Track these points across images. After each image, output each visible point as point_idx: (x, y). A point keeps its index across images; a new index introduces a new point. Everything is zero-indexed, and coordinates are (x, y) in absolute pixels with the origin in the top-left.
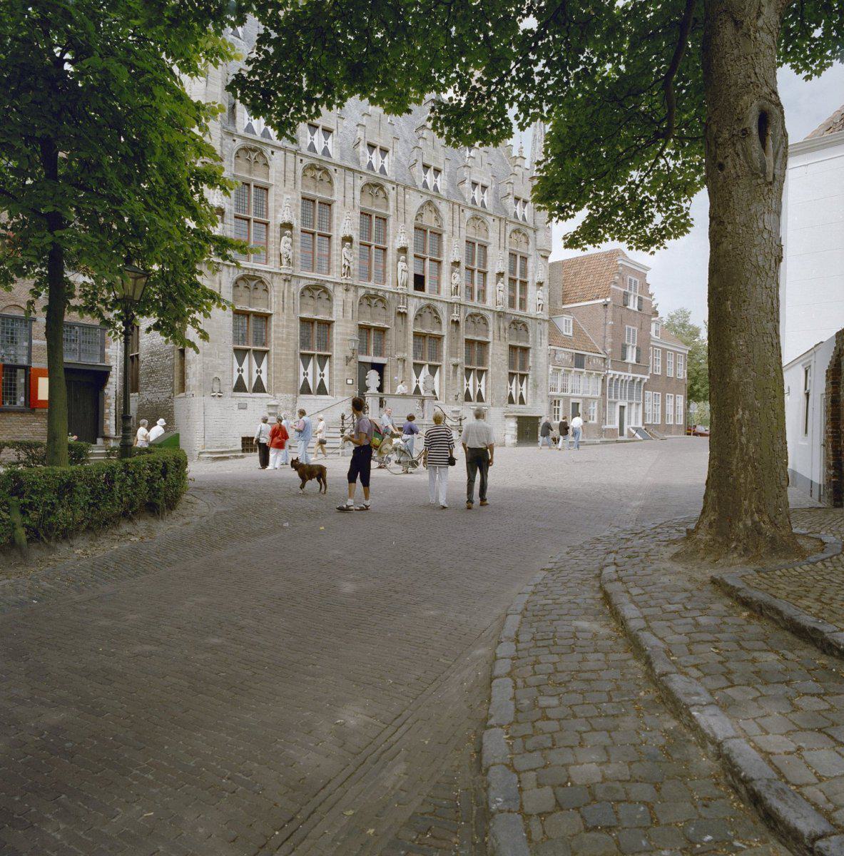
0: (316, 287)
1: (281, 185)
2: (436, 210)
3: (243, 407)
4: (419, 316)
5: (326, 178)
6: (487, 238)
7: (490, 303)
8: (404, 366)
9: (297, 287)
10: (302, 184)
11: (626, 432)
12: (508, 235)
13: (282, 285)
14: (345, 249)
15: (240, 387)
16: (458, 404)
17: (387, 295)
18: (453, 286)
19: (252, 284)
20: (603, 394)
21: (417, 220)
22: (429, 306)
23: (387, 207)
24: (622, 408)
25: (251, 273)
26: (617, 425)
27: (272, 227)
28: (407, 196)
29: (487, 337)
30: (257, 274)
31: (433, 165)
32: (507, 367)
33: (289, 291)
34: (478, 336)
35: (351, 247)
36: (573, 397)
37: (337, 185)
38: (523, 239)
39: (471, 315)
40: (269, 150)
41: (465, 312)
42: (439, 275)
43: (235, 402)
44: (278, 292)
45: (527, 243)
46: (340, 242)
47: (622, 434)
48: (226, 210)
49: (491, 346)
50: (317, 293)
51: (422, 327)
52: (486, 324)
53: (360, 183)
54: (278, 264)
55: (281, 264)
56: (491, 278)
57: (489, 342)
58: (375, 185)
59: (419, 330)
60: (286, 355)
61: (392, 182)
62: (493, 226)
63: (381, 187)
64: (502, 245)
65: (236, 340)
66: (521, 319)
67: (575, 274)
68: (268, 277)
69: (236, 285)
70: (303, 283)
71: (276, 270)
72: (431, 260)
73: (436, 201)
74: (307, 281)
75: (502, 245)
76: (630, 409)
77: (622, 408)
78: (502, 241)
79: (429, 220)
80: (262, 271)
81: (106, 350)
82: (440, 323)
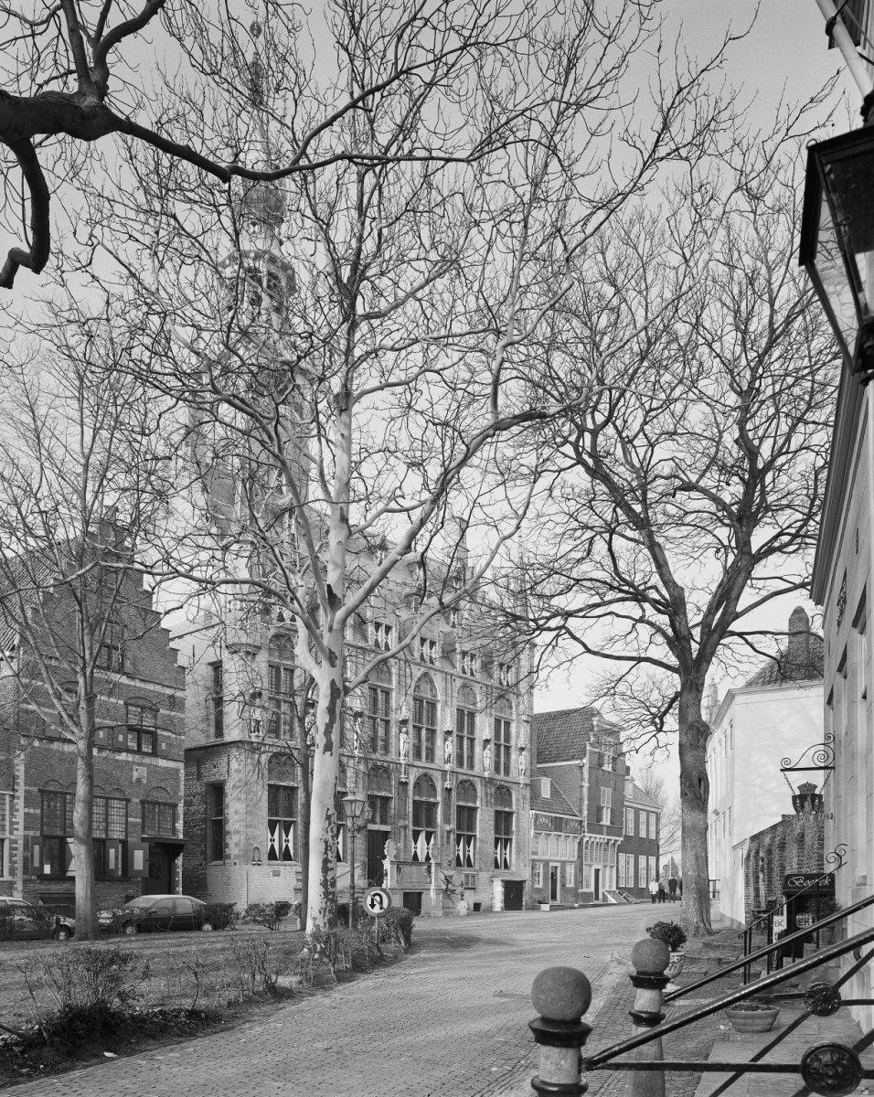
3: (276, 874)
4: (417, 784)
7: (477, 770)
11: (601, 896)
15: (272, 856)
20: (580, 857)
22: (425, 775)
24: (597, 871)
26: (592, 889)
34: (468, 802)
43: (270, 869)
47: (597, 898)
51: (419, 795)
52: (475, 790)
59: (417, 798)
76: (604, 872)
77: (597, 871)
82: (435, 790)
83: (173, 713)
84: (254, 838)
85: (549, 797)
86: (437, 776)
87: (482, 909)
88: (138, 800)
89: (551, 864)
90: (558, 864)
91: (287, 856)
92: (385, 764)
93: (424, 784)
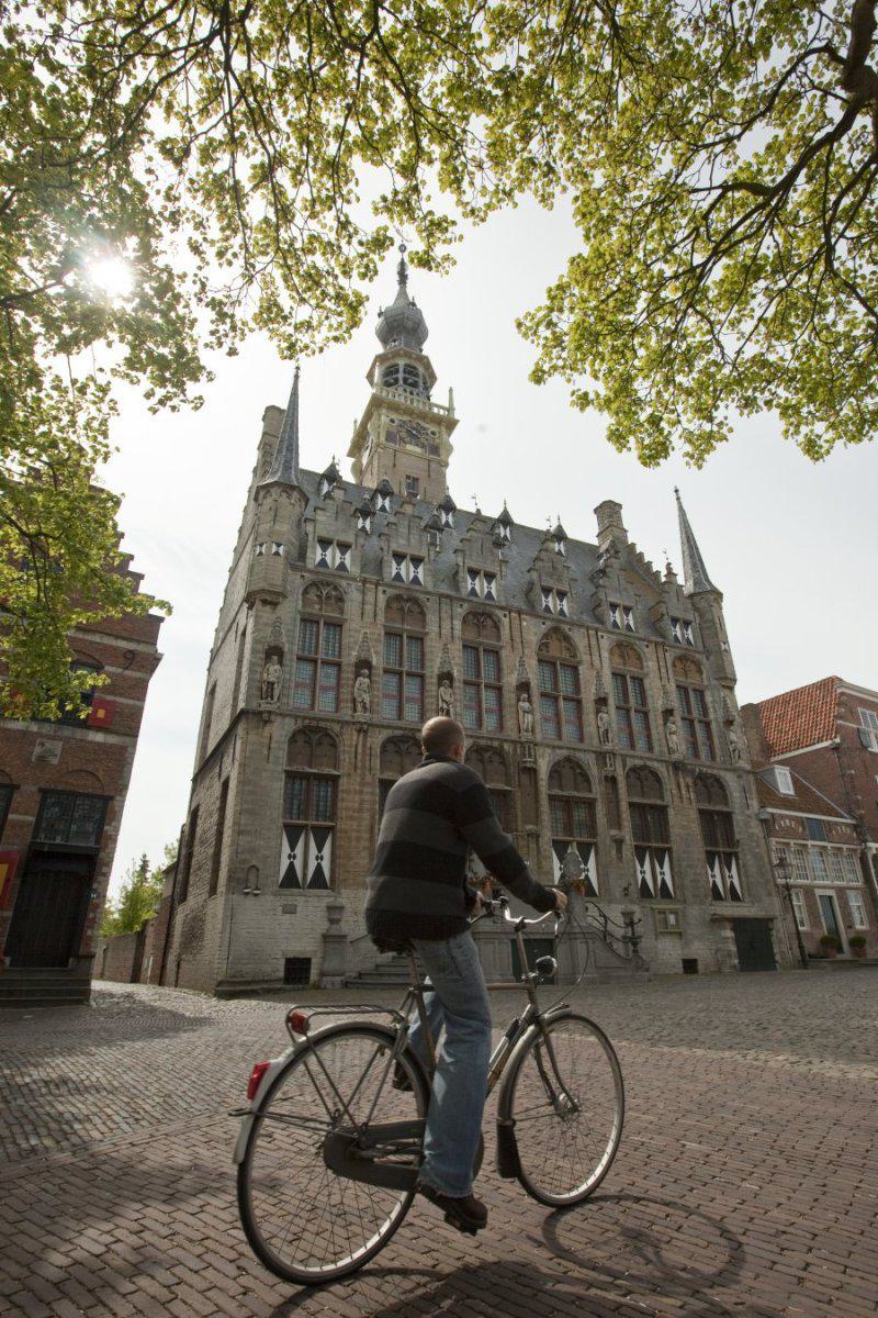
0: (403, 739)
1: (358, 619)
2: (567, 638)
3: (290, 910)
4: (555, 772)
5: (416, 609)
6: (642, 668)
8: (538, 844)
9: (377, 739)
10: (386, 617)
12: (669, 665)
13: (355, 738)
14: (442, 689)
15: (290, 880)
16: (632, 902)
17: (506, 746)
18: (601, 730)
19: (315, 738)
21: (540, 649)
22: (568, 759)
23: (499, 638)
25: (314, 723)
27: (344, 668)
28: (524, 624)
29: (662, 798)
30: (322, 724)
31: (557, 586)
32: (701, 843)
33: (364, 745)
35: (451, 686)
36: (818, 887)
37: (432, 618)
38: (693, 667)
39: (634, 769)
40: (344, 583)
41: (624, 766)
42: (580, 718)
43: (279, 903)
44: (350, 746)
45: (701, 672)
46: (435, 680)
48: (286, 650)
49: (671, 812)
50: (404, 747)
51: (561, 787)
52: (658, 779)
53: (460, 611)
54: (350, 712)
55: (355, 710)
56: (656, 720)
57: (666, 807)
58: (483, 614)
59: (557, 792)
60: (358, 831)
61: (502, 608)
62: (649, 653)
63: (490, 616)
64: (664, 675)
65: (288, 811)
66: (709, 771)
67: (779, 717)
68: (337, 728)
69: (293, 740)
70: (385, 734)
71: (347, 718)
72: (565, 699)
73: (566, 628)
74: (390, 731)
75: (664, 675)
78: (663, 670)
79: (556, 650)
80: (327, 720)
81: (106, 828)
82: (588, 781)
83: (127, 672)
84: (253, 851)
85: (792, 792)
86: (589, 761)
87: (700, 967)
88: (34, 789)
89: (818, 892)
90: (831, 893)
91: (318, 881)
92: (496, 744)
93: (566, 771)
